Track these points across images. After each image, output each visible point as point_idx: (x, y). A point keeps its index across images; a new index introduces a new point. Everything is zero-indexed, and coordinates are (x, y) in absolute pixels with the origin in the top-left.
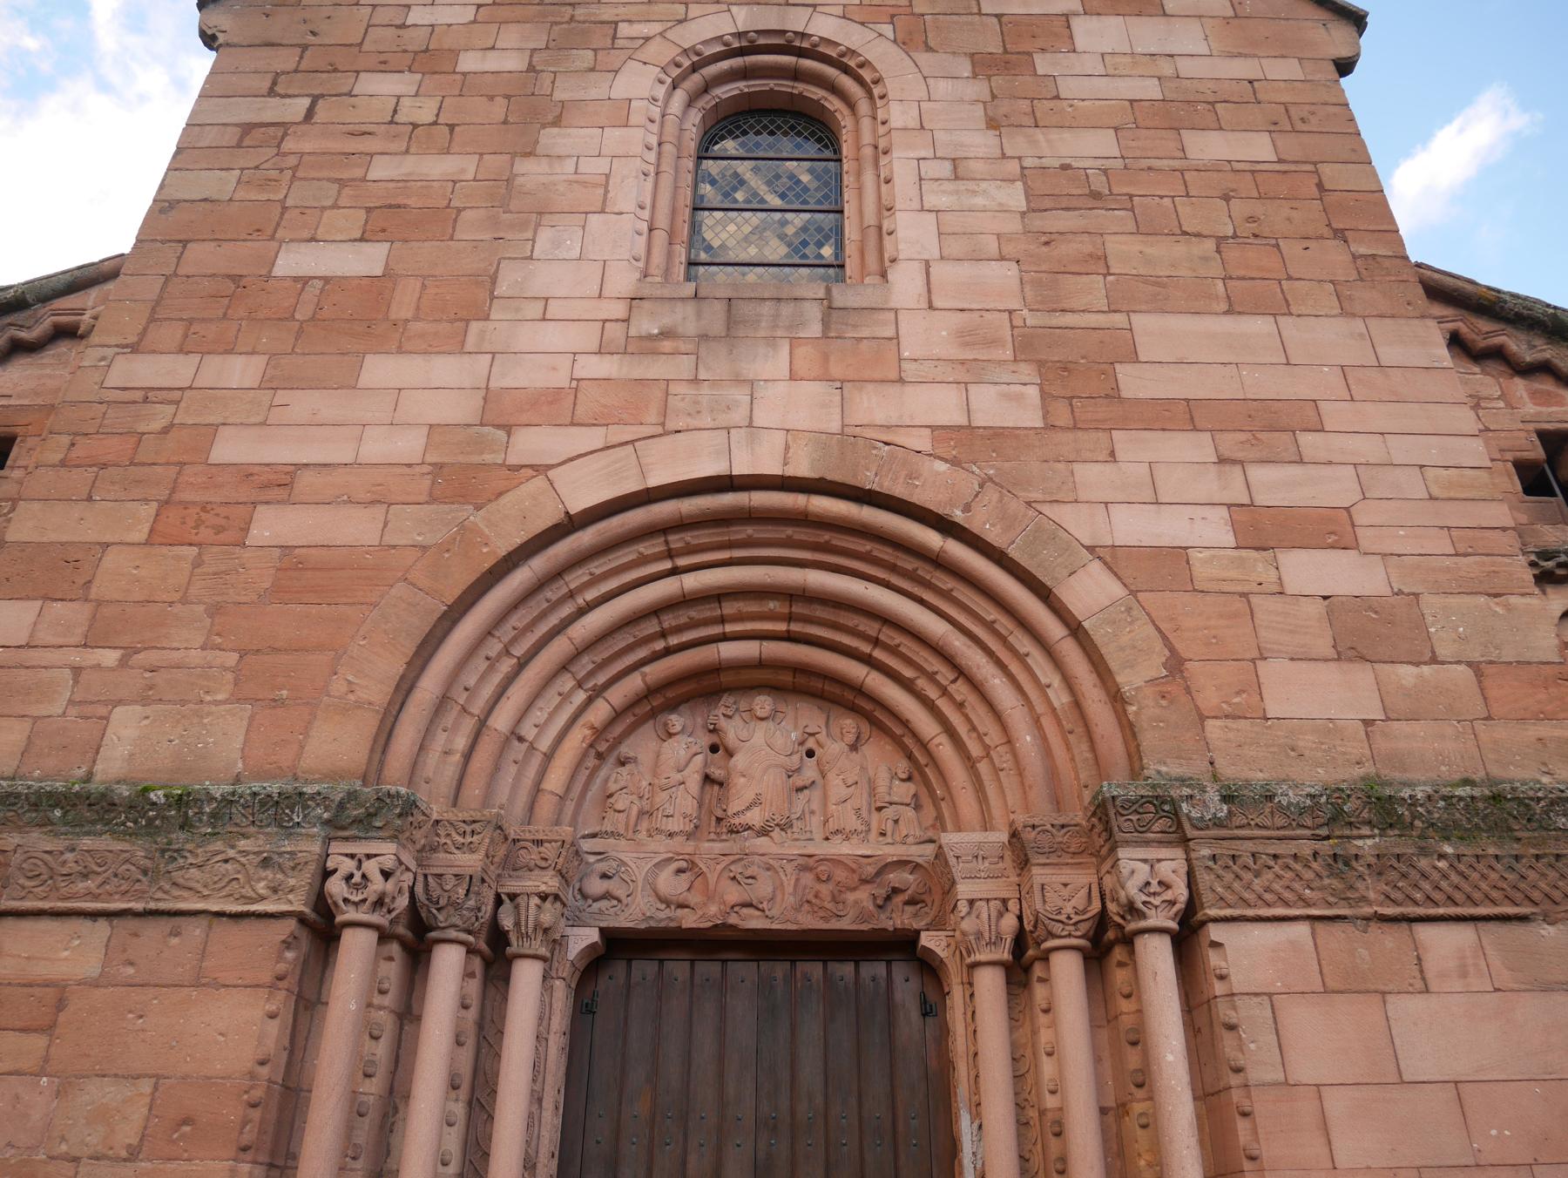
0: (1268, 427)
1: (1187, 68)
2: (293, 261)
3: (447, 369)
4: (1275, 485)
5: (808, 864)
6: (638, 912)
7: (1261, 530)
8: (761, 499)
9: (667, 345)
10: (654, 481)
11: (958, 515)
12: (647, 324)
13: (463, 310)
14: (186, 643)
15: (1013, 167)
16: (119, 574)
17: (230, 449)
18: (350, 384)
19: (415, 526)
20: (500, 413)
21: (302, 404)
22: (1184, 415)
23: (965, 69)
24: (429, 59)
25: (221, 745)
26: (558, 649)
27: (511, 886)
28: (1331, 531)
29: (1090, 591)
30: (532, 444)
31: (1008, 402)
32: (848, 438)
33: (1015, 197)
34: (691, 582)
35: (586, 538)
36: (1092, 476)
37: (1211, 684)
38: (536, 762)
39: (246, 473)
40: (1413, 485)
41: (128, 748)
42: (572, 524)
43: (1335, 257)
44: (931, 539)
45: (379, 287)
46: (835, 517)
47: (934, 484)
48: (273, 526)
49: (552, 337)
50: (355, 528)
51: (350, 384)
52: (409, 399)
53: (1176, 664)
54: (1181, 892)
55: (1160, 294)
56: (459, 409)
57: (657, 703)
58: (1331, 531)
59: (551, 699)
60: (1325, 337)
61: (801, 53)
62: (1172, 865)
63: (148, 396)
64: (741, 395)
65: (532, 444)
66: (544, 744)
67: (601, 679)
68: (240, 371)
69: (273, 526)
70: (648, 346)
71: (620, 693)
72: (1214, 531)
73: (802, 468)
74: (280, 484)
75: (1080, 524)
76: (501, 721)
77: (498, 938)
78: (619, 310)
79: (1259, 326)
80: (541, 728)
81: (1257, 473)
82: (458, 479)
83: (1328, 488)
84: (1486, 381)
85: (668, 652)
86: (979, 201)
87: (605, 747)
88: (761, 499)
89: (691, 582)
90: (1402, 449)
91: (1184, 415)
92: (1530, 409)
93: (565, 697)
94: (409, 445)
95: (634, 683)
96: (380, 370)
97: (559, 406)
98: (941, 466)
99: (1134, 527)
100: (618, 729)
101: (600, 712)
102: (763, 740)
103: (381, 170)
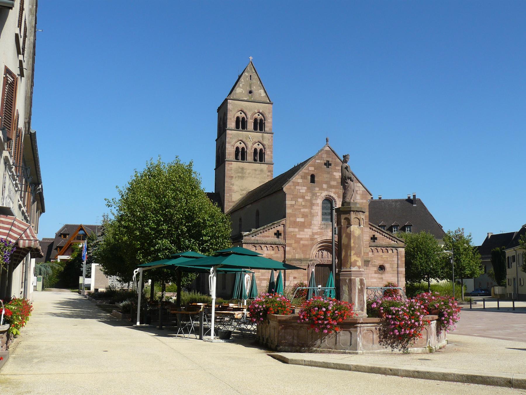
2: (298, 220)
3: (310, 230)
6: (318, 263)
13: (310, 225)
14: (299, 250)
16: (294, 245)
17: (298, 236)
18: (304, 231)
19: (310, 242)
20: (314, 234)
21: (301, 233)
24: (303, 197)
25: (302, 256)
30: (316, 236)
39: (299, 238)
41: (297, 256)
45: (304, 223)
48: (302, 242)
49: (316, 228)
50: (306, 242)
51: (304, 231)
56: (311, 234)
63: (292, 232)
65: (316, 236)
68: (297, 230)
70: (321, 229)
74: (301, 239)
82: (312, 239)
84: (371, 230)
94: (308, 236)
96: (306, 230)
97: (317, 233)
102: (325, 253)
103: (302, 210)
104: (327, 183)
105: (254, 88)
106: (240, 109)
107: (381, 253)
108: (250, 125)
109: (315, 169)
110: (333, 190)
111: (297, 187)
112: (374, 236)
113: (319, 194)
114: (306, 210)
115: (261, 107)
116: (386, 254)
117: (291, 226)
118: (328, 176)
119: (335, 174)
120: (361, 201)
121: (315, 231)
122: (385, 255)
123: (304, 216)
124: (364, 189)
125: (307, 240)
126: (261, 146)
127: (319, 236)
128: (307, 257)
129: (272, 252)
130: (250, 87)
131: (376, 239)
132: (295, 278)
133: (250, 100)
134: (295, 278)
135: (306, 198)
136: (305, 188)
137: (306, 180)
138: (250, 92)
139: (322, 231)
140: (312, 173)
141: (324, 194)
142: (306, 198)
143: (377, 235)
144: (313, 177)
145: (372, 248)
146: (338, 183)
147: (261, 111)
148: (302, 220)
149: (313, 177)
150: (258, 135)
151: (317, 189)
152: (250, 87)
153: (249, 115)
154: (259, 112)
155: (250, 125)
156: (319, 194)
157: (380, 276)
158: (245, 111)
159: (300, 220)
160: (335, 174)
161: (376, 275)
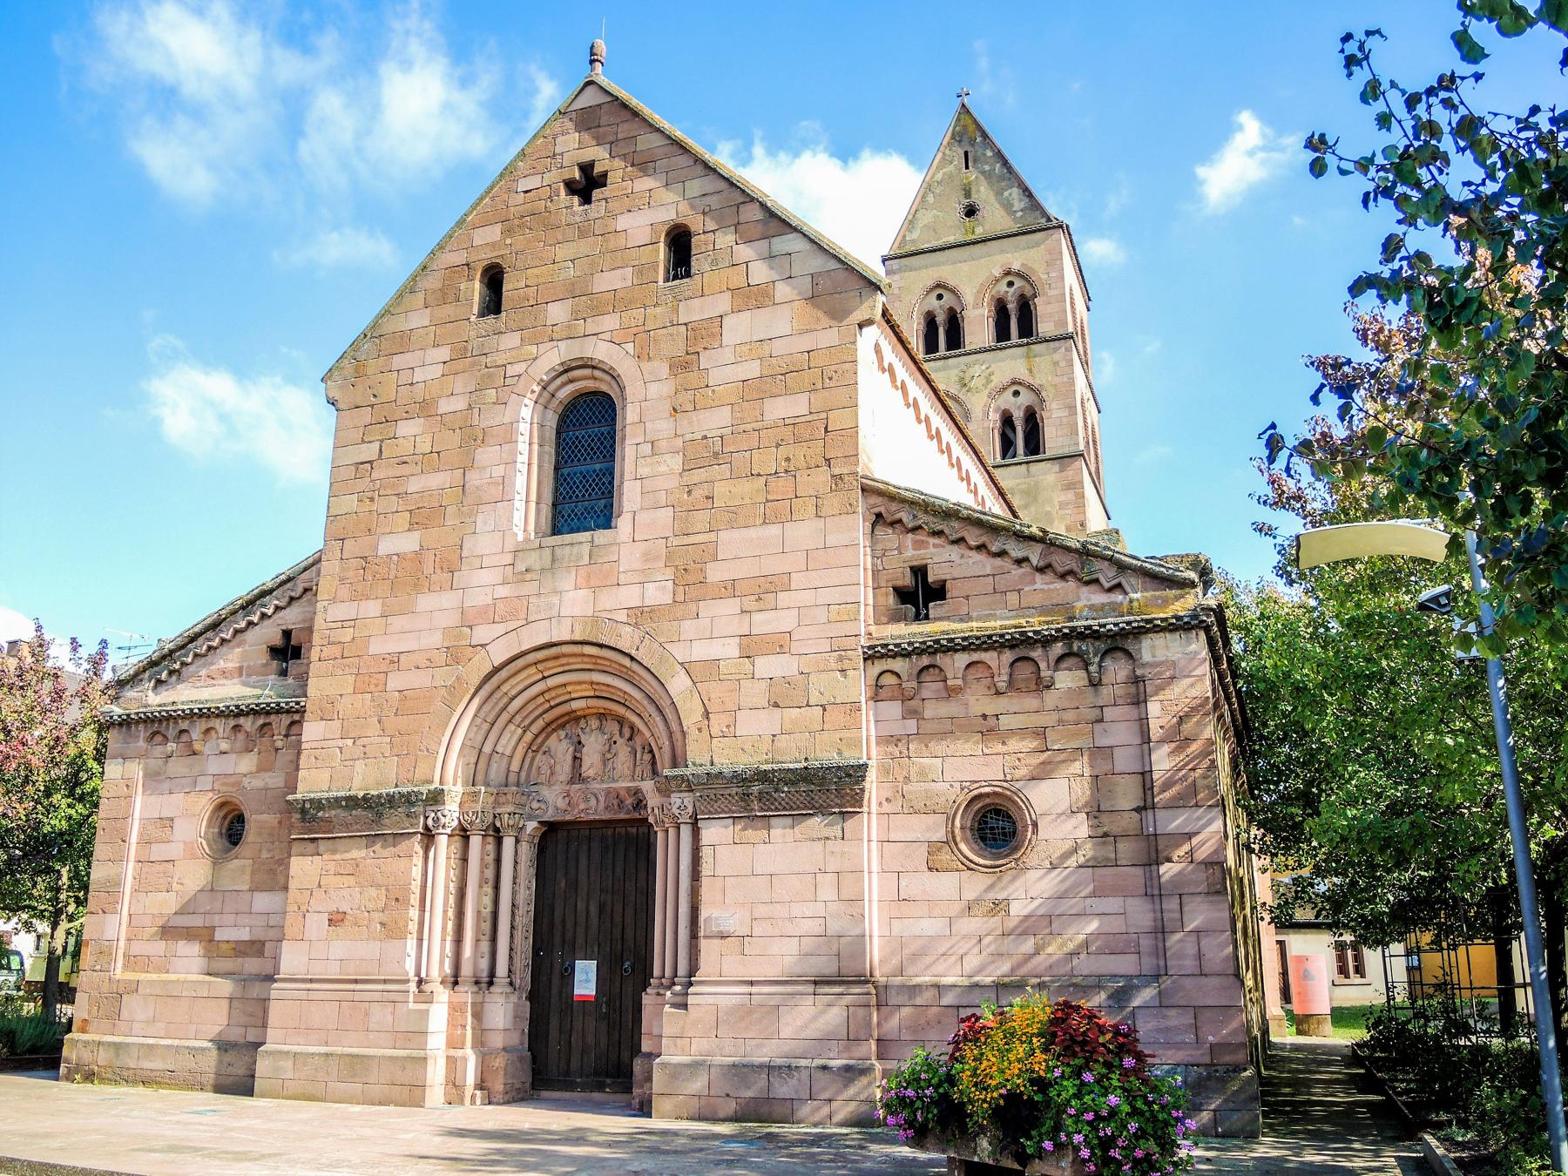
0: (767, 590)
1: (779, 347)
2: (387, 546)
3: (448, 600)
4: (764, 623)
5: (608, 792)
7: (751, 648)
8: (565, 649)
9: (528, 577)
10: (524, 648)
11: (633, 653)
12: (521, 567)
13: (452, 565)
15: (679, 442)
17: (377, 647)
19: (444, 677)
21: (397, 622)
22: (731, 588)
23: (664, 370)
24: (425, 408)
26: (505, 717)
27: (499, 811)
28: (780, 644)
29: (678, 684)
30: (482, 634)
31: (658, 593)
32: (595, 620)
33: (676, 463)
34: (551, 682)
35: (504, 673)
36: (688, 627)
37: (717, 724)
38: (506, 759)
40: (822, 615)
42: (496, 670)
43: (822, 477)
44: (627, 662)
46: (591, 651)
47: (626, 639)
48: (396, 681)
49: (486, 577)
50: (419, 680)
52: (437, 609)
53: (707, 714)
54: (690, 810)
55: (734, 518)
56: (452, 619)
57: (551, 728)
58: (780, 644)
59: (507, 735)
60: (804, 532)
61: (594, 367)
62: (688, 799)
64: (555, 600)
66: (508, 752)
67: (527, 722)
68: (372, 608)
69: (396, 681)
71: (535, 729)
72: (730, 649)
73: (577, 637)
74: (395, 660)
75: (679, 652)
76: (487, 749)
77: (497, 830)
78: (508, 559)
79: (774, 530)
80: (505, 747)
81: (757, 617)
82: (454, 655)
83: (782, 621)
85: (552, 707)
86: (663, 468)
87: (534, 748)
88: (565, 649)
89: (551, 682)
90: (825, 596)
91: (731, 588)
92: (910, 553)
93: (513, 733)
94: (436, 639)
95: (540, 723)
96: (425, 602)
97: (489, 614)
98: (629, 629)
99: (700, 651)
100: (540, 740)
101: (529, 737)
103: (414, 486)
104: (575, 291)
105: (983, 195)
106: (930, 283)
107: (978, 702)
108: (978, 329)
109: (508, 232)
110: (610, 322)
111: (398, 361)
112: (920, 572)
113: (519, 368)
114: (435, 481)
115: (1016, 256)
116: (1031, 702)
117: (344, 592)
118: (584, 247)
119: (623, 222)
120: (806, 342)
121: (478, 598)
122: (1016, 710)
123: (419, 519)
124: (818, 263)
125: (431, 664)
126: (1026, 398)
127: (500, 629)
128: (420, 774)
129: (247, 763)
130: (968, 194)
131: (938, 592)
132: (336, 920)
133: (971, 237)
134: (336, 920)
135: (445, 406)
136: (444, 353)
137: (449, 311)
138: (971, 212)
139: (530, 588)
140: (484, 257)
141: (552, 357)
142: (445, 406)
143: (943, 560)
144: (494, 278)
145: (898, 665)
146: (640, 270)
147: (1016, 266)
148: (407, 543)
149: (494, 278)
150: (1011, 363)
151: (511, 340)
152: (968, 194)
153: (968, 296)
154: (1008, 273)
155: (978, 329)
156: (519, 368)
157: (975, 885)
158: (951, 282)
159: (399, 542)
160: (623, 222)
161: (946, 885)
